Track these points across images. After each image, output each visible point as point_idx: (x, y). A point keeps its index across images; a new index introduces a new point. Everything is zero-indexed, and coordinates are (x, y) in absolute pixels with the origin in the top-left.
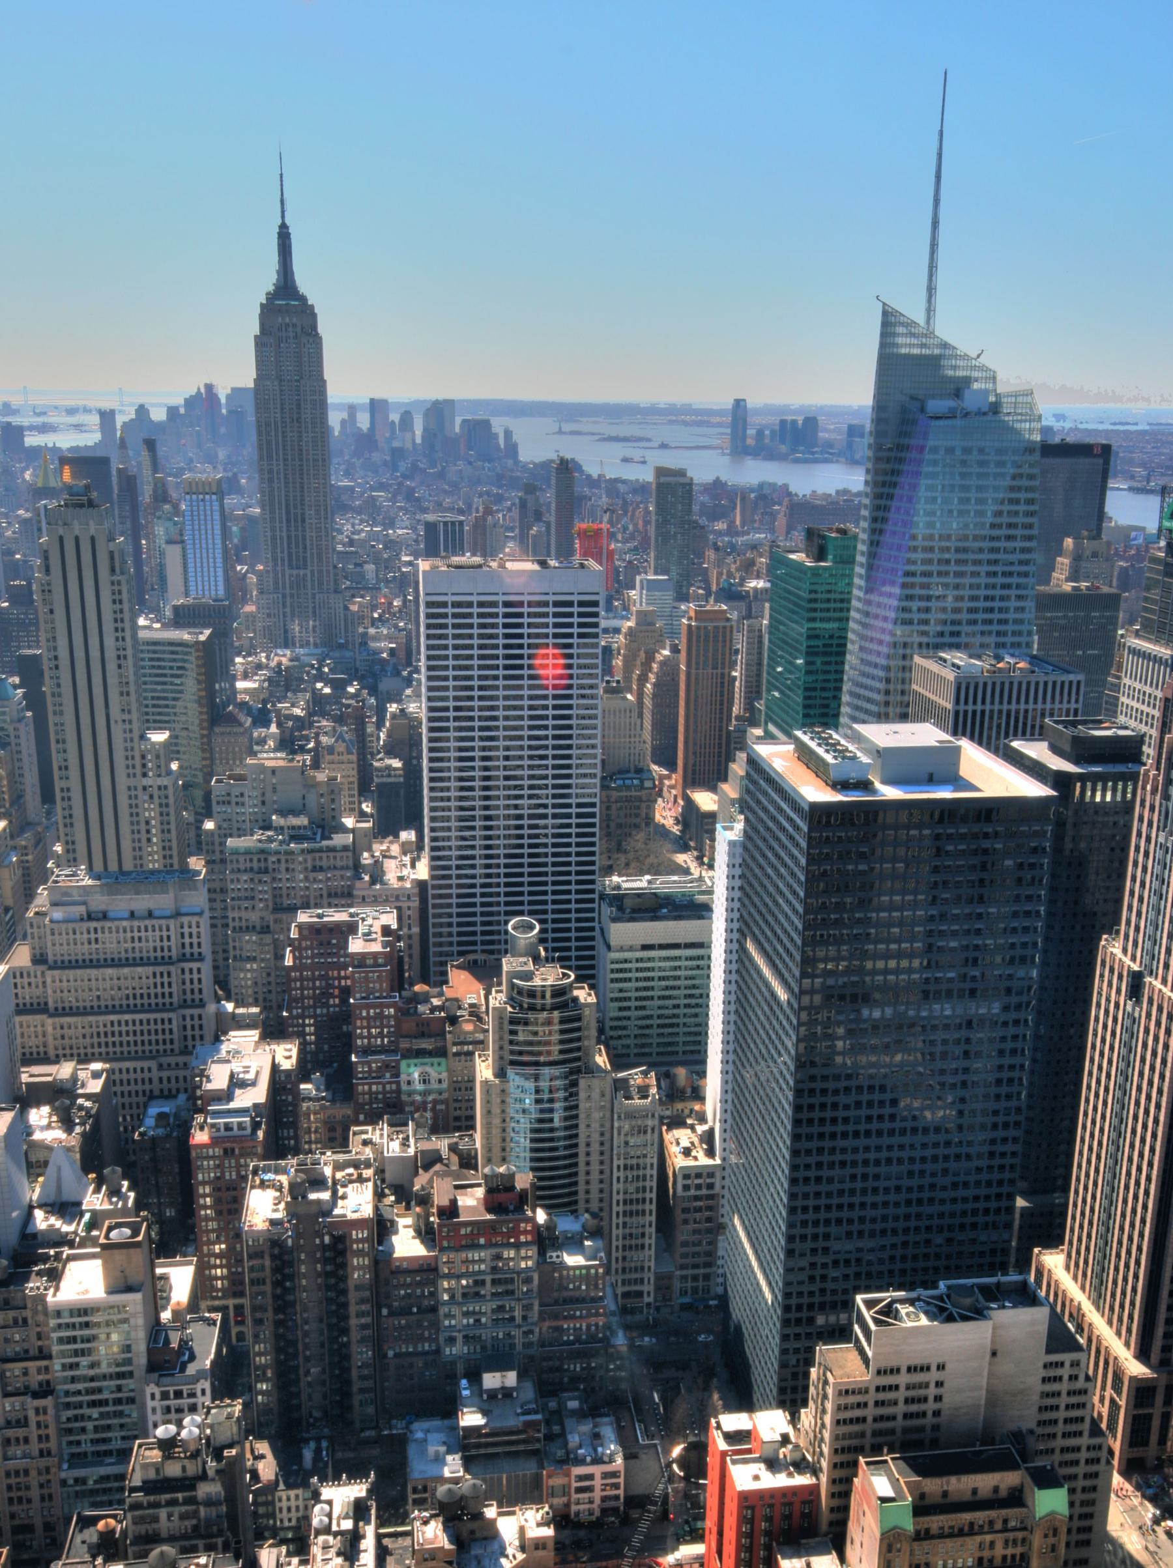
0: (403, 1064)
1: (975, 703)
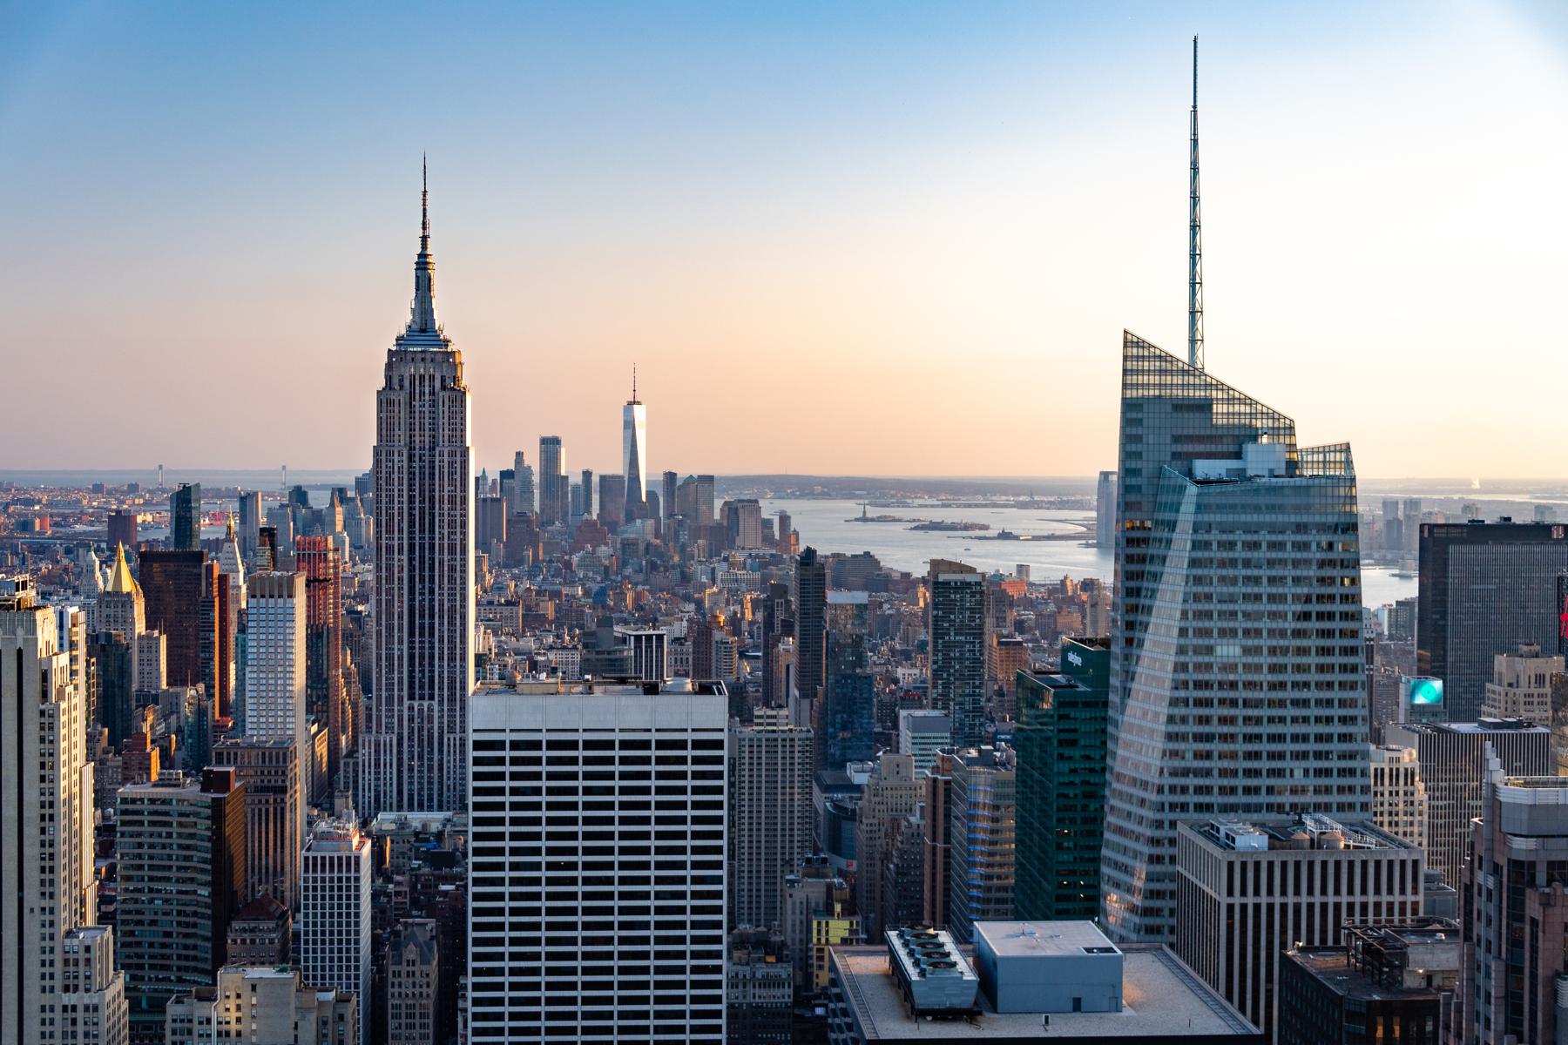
1: (1257, 893)
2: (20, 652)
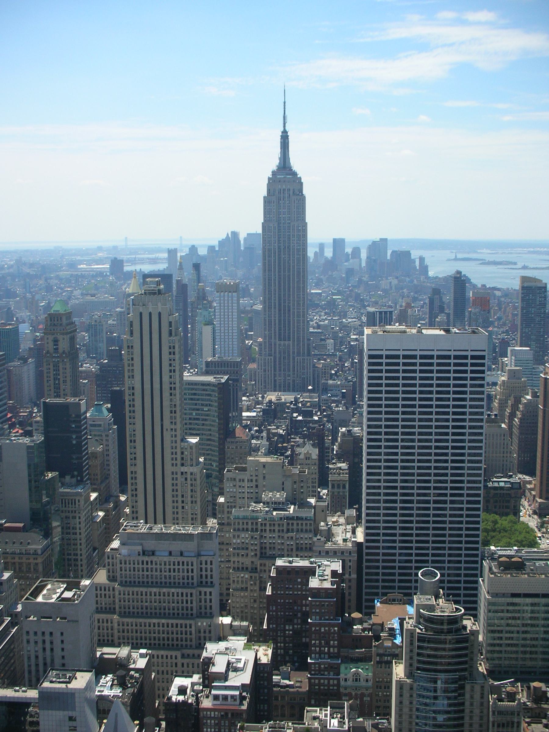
0: (342, 667)
2: (160, 314)
